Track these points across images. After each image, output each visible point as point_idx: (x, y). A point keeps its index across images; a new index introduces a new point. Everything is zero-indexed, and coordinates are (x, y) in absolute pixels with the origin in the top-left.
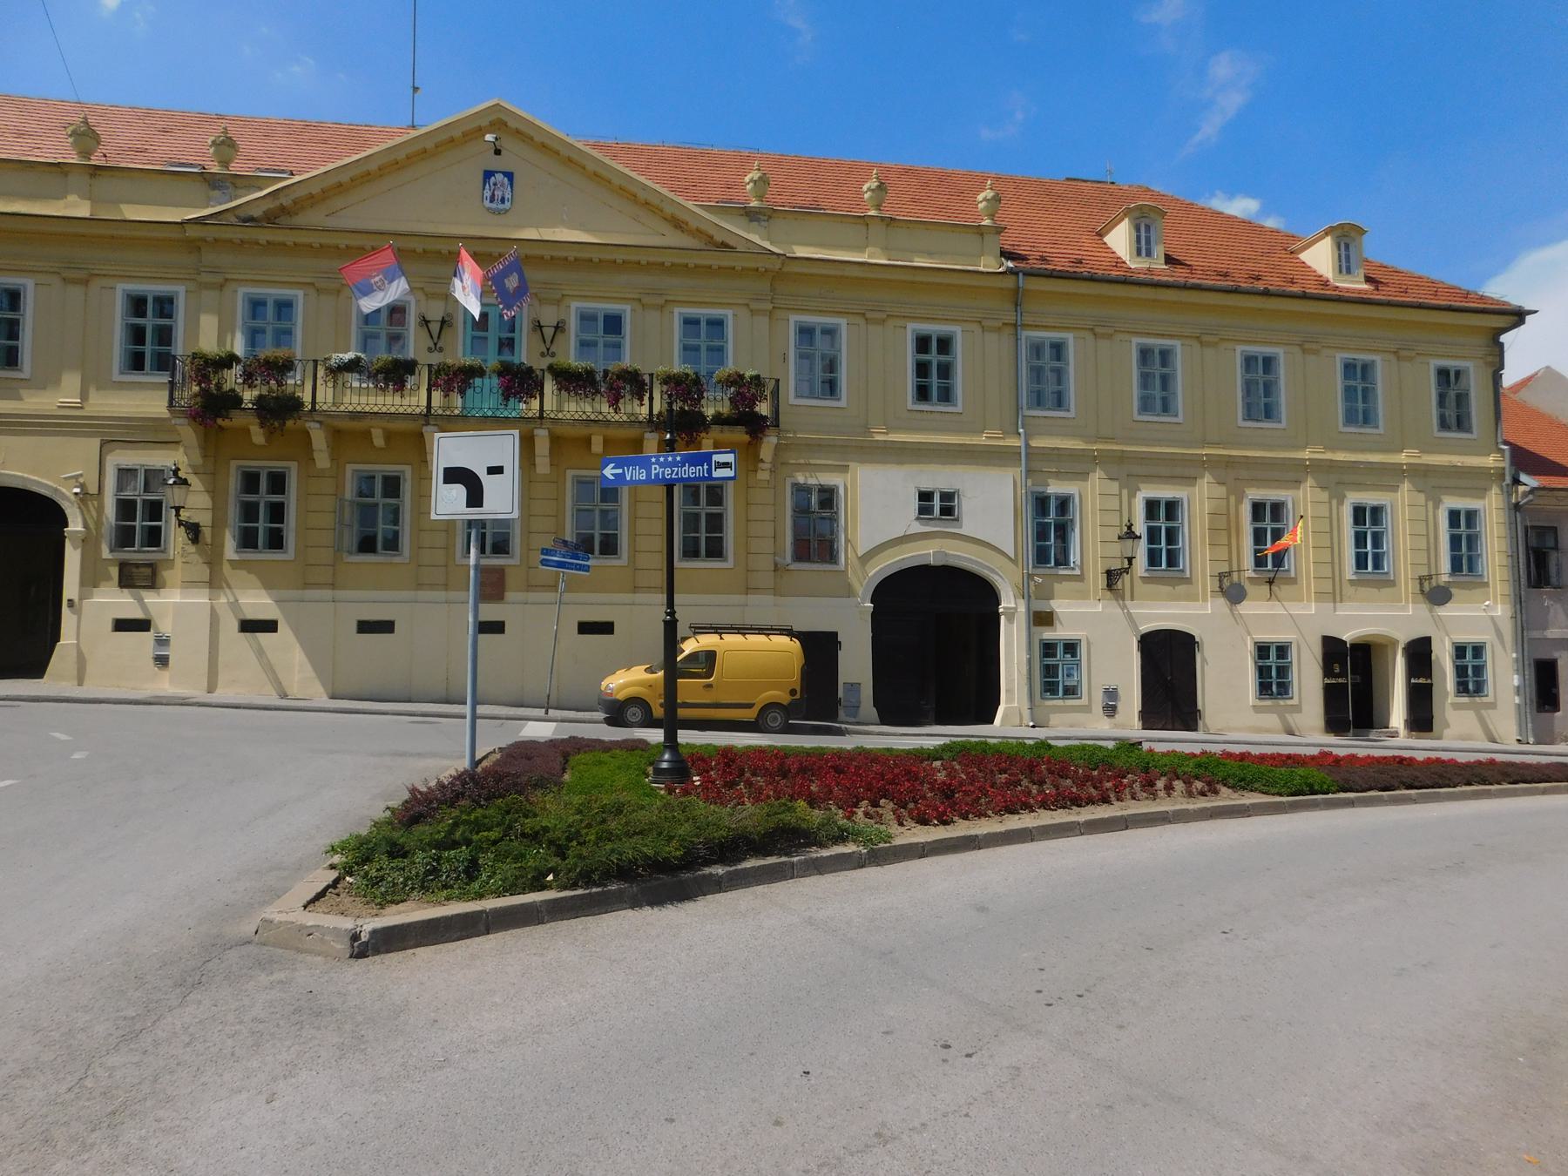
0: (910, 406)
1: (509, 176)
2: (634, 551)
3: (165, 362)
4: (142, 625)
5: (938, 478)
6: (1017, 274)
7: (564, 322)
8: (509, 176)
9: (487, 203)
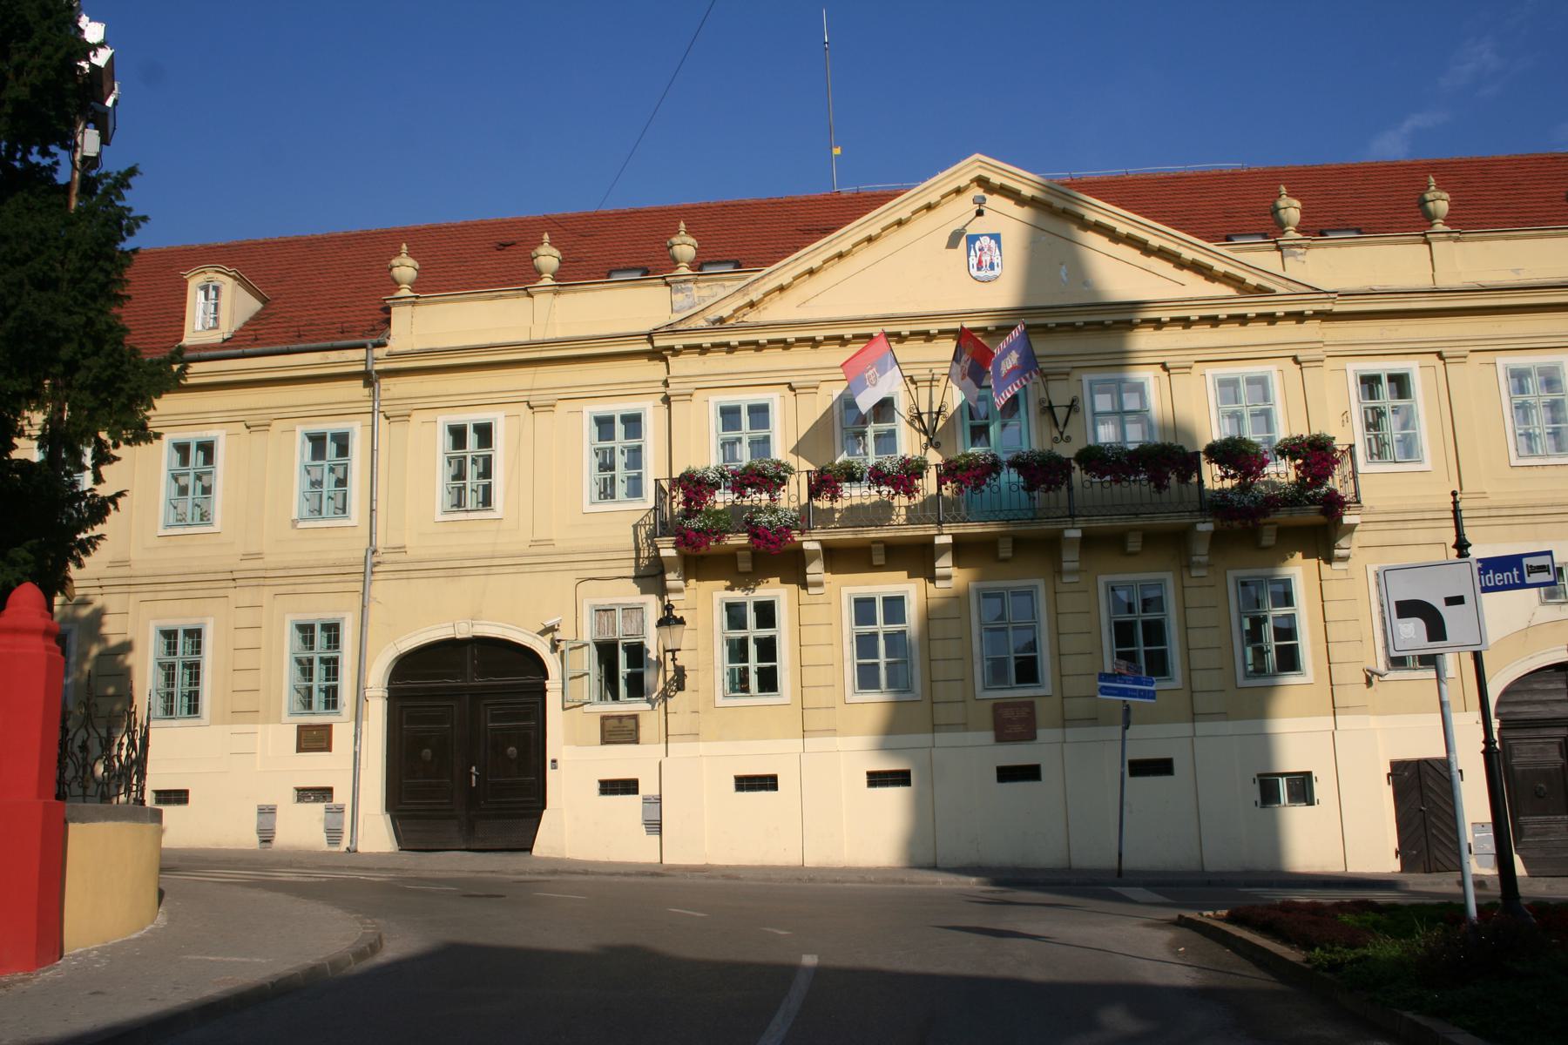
1: (996, 237)
2: (1189, 670)
4: (627, 787)
8: (996, 237)
9: (974, 272)
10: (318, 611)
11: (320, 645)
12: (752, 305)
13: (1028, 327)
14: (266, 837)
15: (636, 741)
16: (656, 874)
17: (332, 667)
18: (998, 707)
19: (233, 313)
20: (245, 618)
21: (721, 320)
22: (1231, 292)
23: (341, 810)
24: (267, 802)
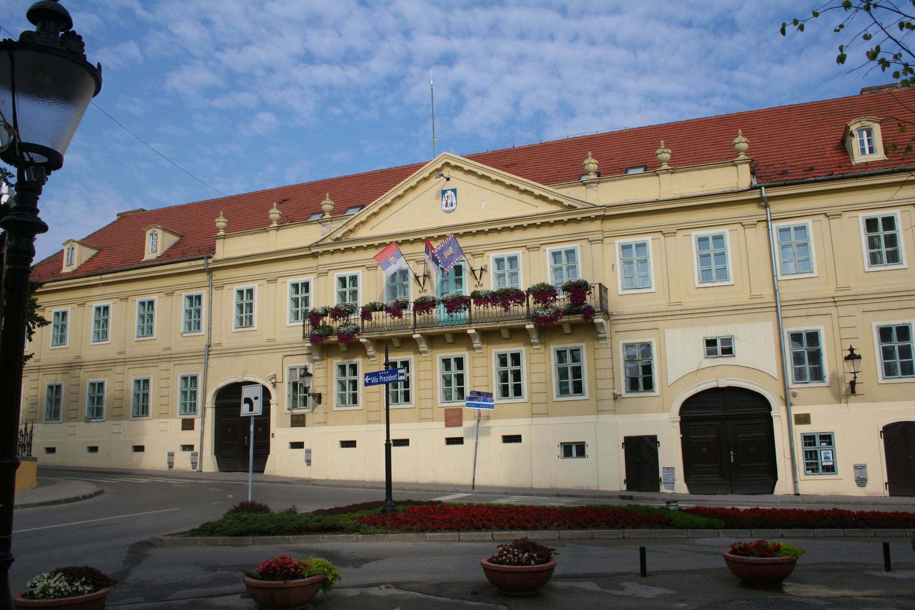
5: (717, 331)
6: (760, 188)
7: (486, 266)
8: (454, 191)
9: (444, 208)
10: (189, 371)
12: (351, 231)
14: (171, 465)
15: (304, 426)
16: (307, 481)
17: (194, 393)
18: (447, 411)
19: (163, 244)
20: (164, 374)
21: (337, 239)
22: (559, 208)
23: (196, 455)
24: (171, 451)
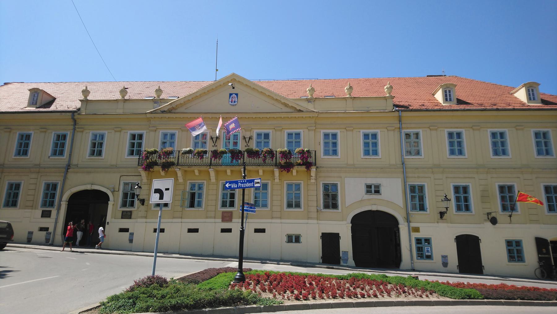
0: (362, 157)
3: (139, 153)
4: (126, 230)
8: (237, 95)
11: (51, 189)
13: (238, 118)
15: (130, 218)
